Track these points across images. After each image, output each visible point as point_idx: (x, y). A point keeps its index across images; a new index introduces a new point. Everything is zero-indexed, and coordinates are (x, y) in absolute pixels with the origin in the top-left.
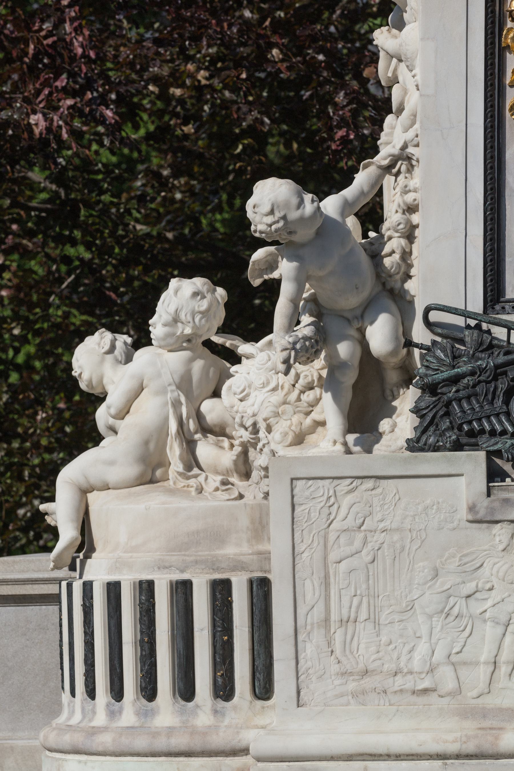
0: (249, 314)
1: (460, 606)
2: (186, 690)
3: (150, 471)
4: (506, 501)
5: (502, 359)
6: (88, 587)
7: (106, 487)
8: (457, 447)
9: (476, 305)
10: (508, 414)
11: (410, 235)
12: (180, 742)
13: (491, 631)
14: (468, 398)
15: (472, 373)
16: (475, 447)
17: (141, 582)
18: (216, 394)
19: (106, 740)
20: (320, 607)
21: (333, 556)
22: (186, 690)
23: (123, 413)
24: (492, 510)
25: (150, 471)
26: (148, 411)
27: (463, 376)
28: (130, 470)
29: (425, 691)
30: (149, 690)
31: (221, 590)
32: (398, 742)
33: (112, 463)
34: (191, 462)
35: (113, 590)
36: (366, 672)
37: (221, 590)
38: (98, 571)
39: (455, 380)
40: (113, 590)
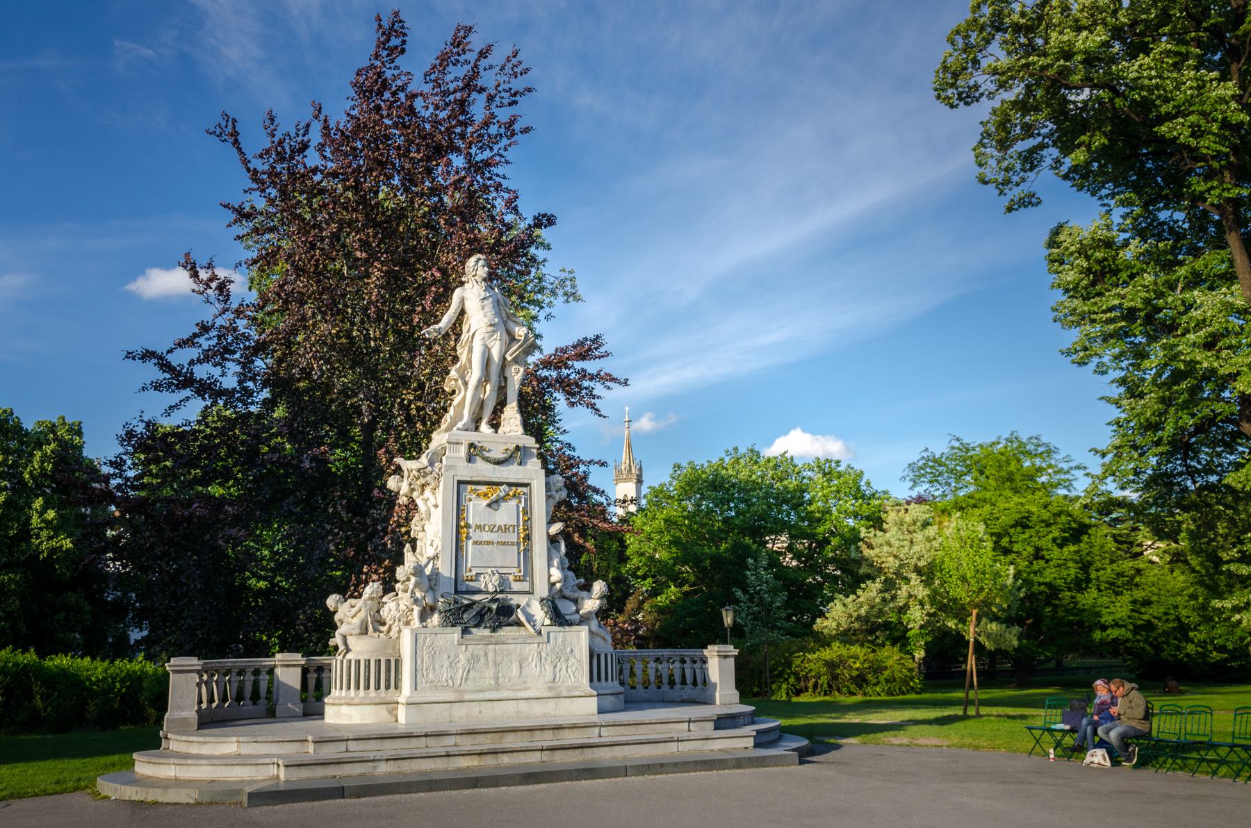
2: (378, 687)
3: (364, 632)
8: (453, 626)
12: (378, 701)
13: (460, 671)
19: (357, 701)
22: (378, 687)
25: (364, 632)
26: (362, 615)
28: (357, 631)
30: (368, 687)
31: (388, 662)
32: (441, 699)
34: (375, 630)
37: (388, 662)
38: (349, 656)
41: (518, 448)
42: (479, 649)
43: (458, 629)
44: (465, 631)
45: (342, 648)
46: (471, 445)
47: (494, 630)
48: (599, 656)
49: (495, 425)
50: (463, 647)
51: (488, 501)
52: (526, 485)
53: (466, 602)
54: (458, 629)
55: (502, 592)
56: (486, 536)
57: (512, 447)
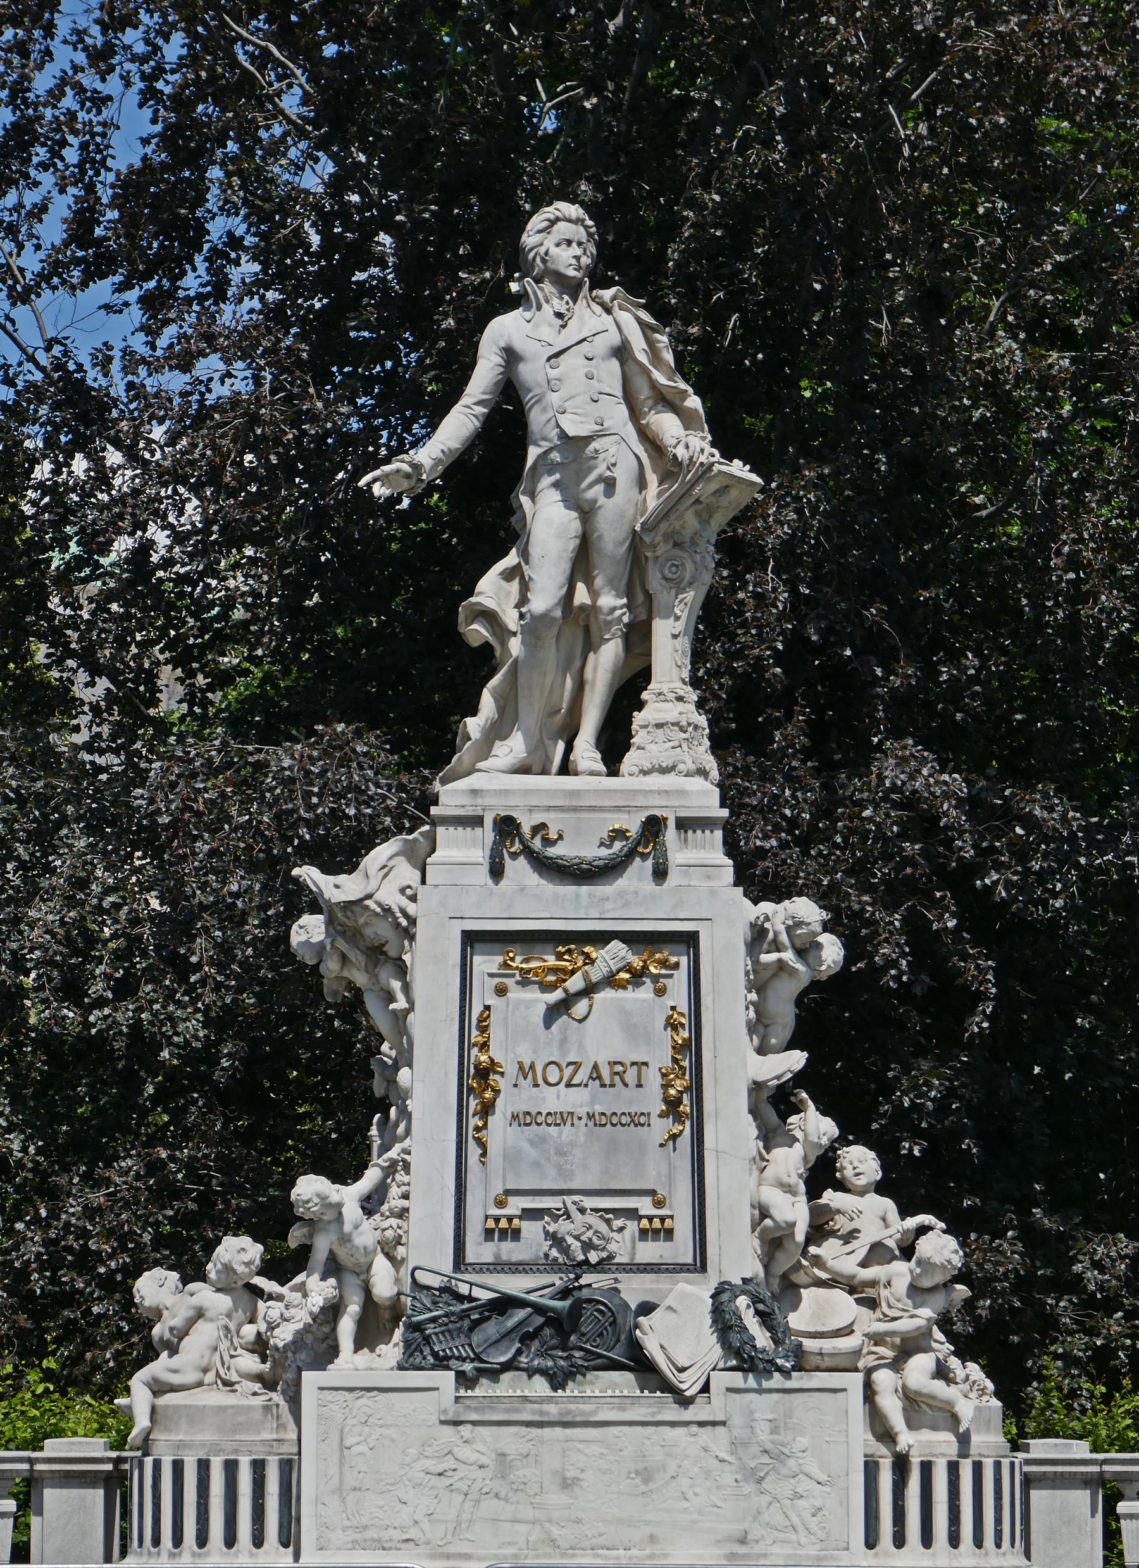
0: (284, 1265)
1: (435, 1481)
4: (468, 1407)
5: (466, 1306)
6: (157, 1464)
7: (174, 1389)
8: (433, 1368)
9: (447, 1266)
10: (470, 1345)
11: (403, 1214)
14: (443, 1333)
15: (446, 1315)
16: (447, 1368)
17: (200, 1461)
18: (252, 1321)
20: (336, 1480)
21: (347, 1443)
22: (230, 1540)
23: (183, 1333)
24: (457, 1413)
27: (439, 1317)
29: (407, 1540)
33: (175, 1371)
35: (178, 1467)
36: (365, 1527)
39: (434, 1320)
40: (178, 1467)
41: (653, 826)
42: (511, 1440)
43: (446, 1379)
44: (464, 1380)
45: (142, 1421)
46: (507, 827)
47: (557, 1381)
48: (927, 1468)
49: (614, 744)
50: (466, 1430)
51: (558, 994)
52: (690, 940)
53: (485, 1295)
54: (446, 1379)
55: (601, 1266)
56: (553, 1100)
57: (633, 825)
